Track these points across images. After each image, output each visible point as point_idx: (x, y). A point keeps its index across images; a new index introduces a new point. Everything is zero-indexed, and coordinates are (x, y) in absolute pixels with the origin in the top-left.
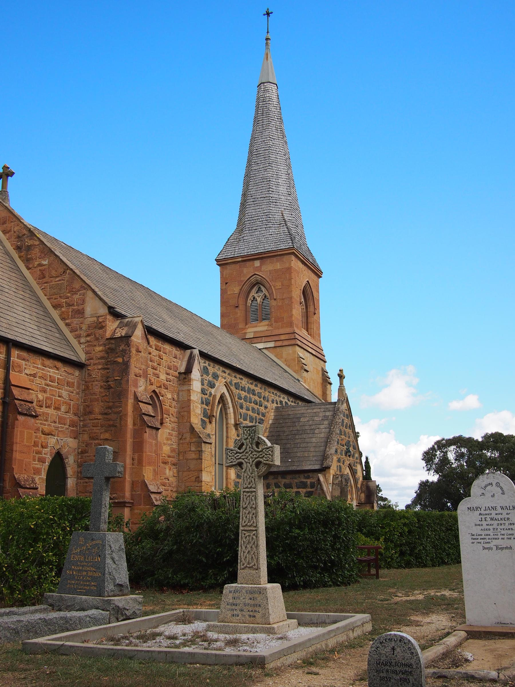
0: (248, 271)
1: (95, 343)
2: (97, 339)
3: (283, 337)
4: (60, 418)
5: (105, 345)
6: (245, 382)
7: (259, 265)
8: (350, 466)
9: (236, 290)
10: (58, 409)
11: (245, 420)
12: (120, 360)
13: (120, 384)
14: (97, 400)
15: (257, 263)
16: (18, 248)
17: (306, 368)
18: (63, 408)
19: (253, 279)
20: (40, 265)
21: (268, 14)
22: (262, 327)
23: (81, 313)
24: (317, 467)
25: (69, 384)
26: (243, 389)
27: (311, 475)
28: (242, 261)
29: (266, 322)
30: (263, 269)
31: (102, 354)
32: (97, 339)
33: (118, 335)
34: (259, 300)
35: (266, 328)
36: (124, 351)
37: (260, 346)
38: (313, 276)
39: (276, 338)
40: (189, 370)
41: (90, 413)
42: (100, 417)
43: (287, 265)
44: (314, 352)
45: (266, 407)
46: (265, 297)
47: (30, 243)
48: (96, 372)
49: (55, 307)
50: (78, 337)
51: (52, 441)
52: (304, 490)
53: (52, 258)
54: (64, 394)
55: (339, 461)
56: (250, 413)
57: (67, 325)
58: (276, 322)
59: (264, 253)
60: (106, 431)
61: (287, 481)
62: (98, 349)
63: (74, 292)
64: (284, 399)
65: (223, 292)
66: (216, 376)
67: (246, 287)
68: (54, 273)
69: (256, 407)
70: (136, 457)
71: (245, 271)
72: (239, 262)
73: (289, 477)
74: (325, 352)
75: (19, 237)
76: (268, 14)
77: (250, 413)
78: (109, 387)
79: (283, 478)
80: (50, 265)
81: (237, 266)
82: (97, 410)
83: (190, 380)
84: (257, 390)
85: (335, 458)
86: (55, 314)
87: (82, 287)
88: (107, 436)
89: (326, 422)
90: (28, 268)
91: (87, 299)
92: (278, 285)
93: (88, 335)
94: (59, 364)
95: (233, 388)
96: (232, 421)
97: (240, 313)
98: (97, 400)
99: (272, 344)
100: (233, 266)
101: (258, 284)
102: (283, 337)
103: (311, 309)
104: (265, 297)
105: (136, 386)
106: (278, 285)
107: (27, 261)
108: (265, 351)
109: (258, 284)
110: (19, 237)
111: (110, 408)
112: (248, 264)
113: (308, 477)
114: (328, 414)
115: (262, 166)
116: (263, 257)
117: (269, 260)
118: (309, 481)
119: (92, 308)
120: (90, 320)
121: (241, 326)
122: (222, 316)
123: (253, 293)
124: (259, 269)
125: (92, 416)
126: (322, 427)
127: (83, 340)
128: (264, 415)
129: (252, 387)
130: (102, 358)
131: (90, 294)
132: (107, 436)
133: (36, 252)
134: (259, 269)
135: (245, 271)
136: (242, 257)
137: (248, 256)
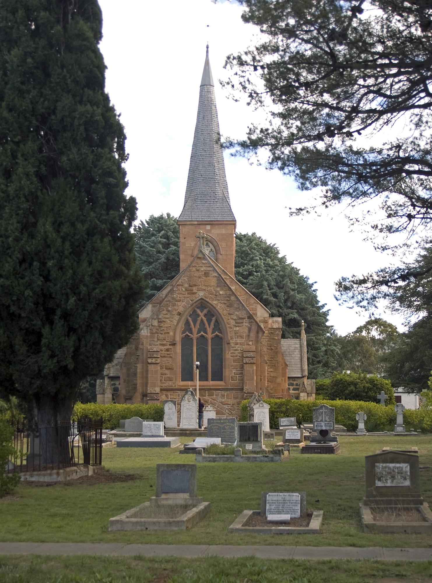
5: (268, 331)
7: (209, 228)
13: (277, 348)
14: (266, 354)
15: (208, 227)
24: (300, 376)
27: (296, 379)
28: (198, 224)
33: (275, 327)
43: (230, 232)
46: (211, 250)
52: (292, 387)
59: (215, 221)
60: (271, 368)
70: (283, 379)
72: (195, 224)
78: (272, 349)
81: (193, 227)
88: (271, 370)
89: (297, 351)
91: (258, 309)
92: (224, 245)
98: (266, 354)
100: (190, 227)
104: (211, 250)
111: (272, 358)
112: (202, 227)
113: (294, 381)
115: (208, 153)
116: (212, 223)
117: (217, 226)
118: (295, 383)
126: (295, 353)
130: (268, 336)
132: (271, 370)
134: (209, 231)
136: (198, 221)
137: (202, 221)
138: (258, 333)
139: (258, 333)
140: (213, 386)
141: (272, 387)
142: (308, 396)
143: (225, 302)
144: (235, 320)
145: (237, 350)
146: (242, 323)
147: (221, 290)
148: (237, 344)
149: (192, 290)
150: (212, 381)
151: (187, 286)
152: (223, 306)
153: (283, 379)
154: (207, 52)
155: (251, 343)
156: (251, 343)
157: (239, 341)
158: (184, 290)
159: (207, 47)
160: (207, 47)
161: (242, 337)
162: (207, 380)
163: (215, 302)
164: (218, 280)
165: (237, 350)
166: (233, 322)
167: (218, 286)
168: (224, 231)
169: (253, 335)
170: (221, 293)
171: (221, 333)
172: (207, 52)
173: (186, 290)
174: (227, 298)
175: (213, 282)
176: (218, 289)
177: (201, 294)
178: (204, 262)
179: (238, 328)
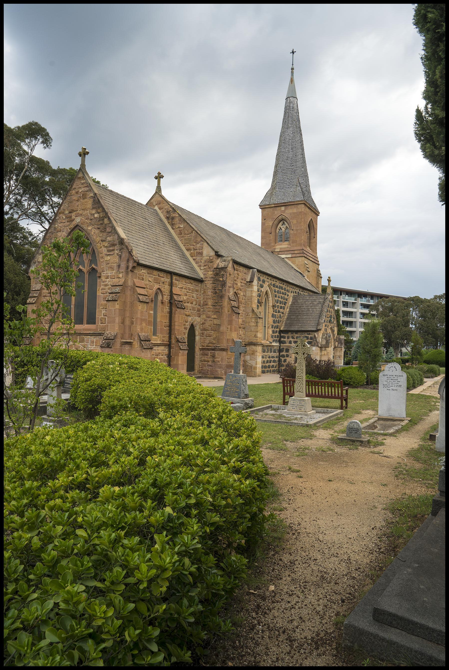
0: (278, 212)
1: (209, 270)
2: (210, 268)
3: (296, 252)
4: (193, 308)
5: (213, 271)
6: (278, 283)
8: (331, 328)
9: (271, 224)
10: (192, 303)
11: (277, 303)
12: (221, 279)
13: (222, 291)
14: (210, 299)
15: (283, 208)
16: (168, 218)
17: (309, 269)
18: (194, 303)
19: (280, 218)
20: (179, 227)
21: (293, 52)
22: (285, 245)
23: (201, 254)
24: (315, 329)
25: (197, 291)
26: (277, 287)
29: (287, 243)
30: (286, 212)
31: (212, 276)
32: (210, 268)
33: (220, 267)
34: (283, 229)
35: (286, 246)
36: (223, 275)
37: (283, 256)
38: (314, 215)
39: (292, 252)
40: (251, 281)
41: (207, 305)
42: (211, 307)
43: (300, 210)
44: (313, 260)
45: (288, 296)
47: (174, 215)
48: (209, 284)
49: (188, 250)
50: (200, 266)
51: (190, 319)
53: (186, 224)
54: (195, 295)
55: (326, 326)
56: (280, 299)
57: (194, 259)
58: (292, 243)
59: (287, 203)
61: (298, 335)
62: (210, 273)
63: (197, 243)
64: (297, 290)
65: (263, 224)
66: (264, 281)
67: (276, 222)
68: (186, 232)
69: (283, 296)
70: (229, 327)
71: (276, 212)
73: (299, 333)
74: (319, 259)
75: (167, 212)
76: (293, 52)
77: (280, 299)
78: (216, 293)
79: (296, 334)
80: (184, 228)
81: (271, 209)
82: (210, 303)
83: (252, 286)
84: (284, 286)
85: (324, 325)
86: (187, 254)
87: (201, 240)
89: (320, 305)
90: (173, 229)
91: (204, 247)
92: (295, 221)
93: (205, 266)
94: (192, 281)
95: (272, 287)
96: (271, 304)
97: (272, 237)
98: (210, 299)
99: (290, 256)
100: (269, 209)
101: (283, 220)
102: (296, 252)
103: (312, 235)
105: (229, 292)
106: (295, 221)
107: (172, 225)
108: (285, 259)
109: (283, 220)
110: (167, 212)
113: (309, 334)
114: (321, 300)
116: (286, 205)
117: (290, 207)
118: (309, 336)
119: (207, 252)
120: (206, 258)
121: (273, 244)
122: (262, 238)
123: (280, 225)
124: (284, 211)
125: (207, 307)
126: (317, 307)
127: (202, 268)
128: (287, 300)
129: (282, 285)
130: (212, 278)
131: (205, 244)
132: (215, 316)
133: (177, 220)
134: (284, 211)
135: (276, 212)
137: (278, 204)
138: (128, 261)
139: (128, 261)
140: (84, 329)
141: (215, 336)
142: (321, 350)
143: (99, 226)
144: (106, 247)
145: (106, 285)
146: (113, 250)
147: (96, 213)
148: (107, 278)
149: (71, 217)
150: (88, 323)
151: (67, 212)
152: (97, 231)
153: (229, 327)
154: (292, 73)
155: (121, 275)
156: (121, 275)
157: (109, 273)
158: (64, 217)
159: (292, 69)
160: (292, 69)
161: (112, 268)
162: (82, 323)
163: (90, 228)
164: (94, 201)
165: (106, 285)
166: (104, 250)
167: (93, 208)
168: (295, 210)
169: (123, 265)
170: (96, 215)
171: (97, 265)
172: (292, 73)
173: (67, 217)
174: (101, 222)
175: (89, 203)
176: (94, 212)
177: (78, 220)
178: (82, 181)
179: (109, 258)
